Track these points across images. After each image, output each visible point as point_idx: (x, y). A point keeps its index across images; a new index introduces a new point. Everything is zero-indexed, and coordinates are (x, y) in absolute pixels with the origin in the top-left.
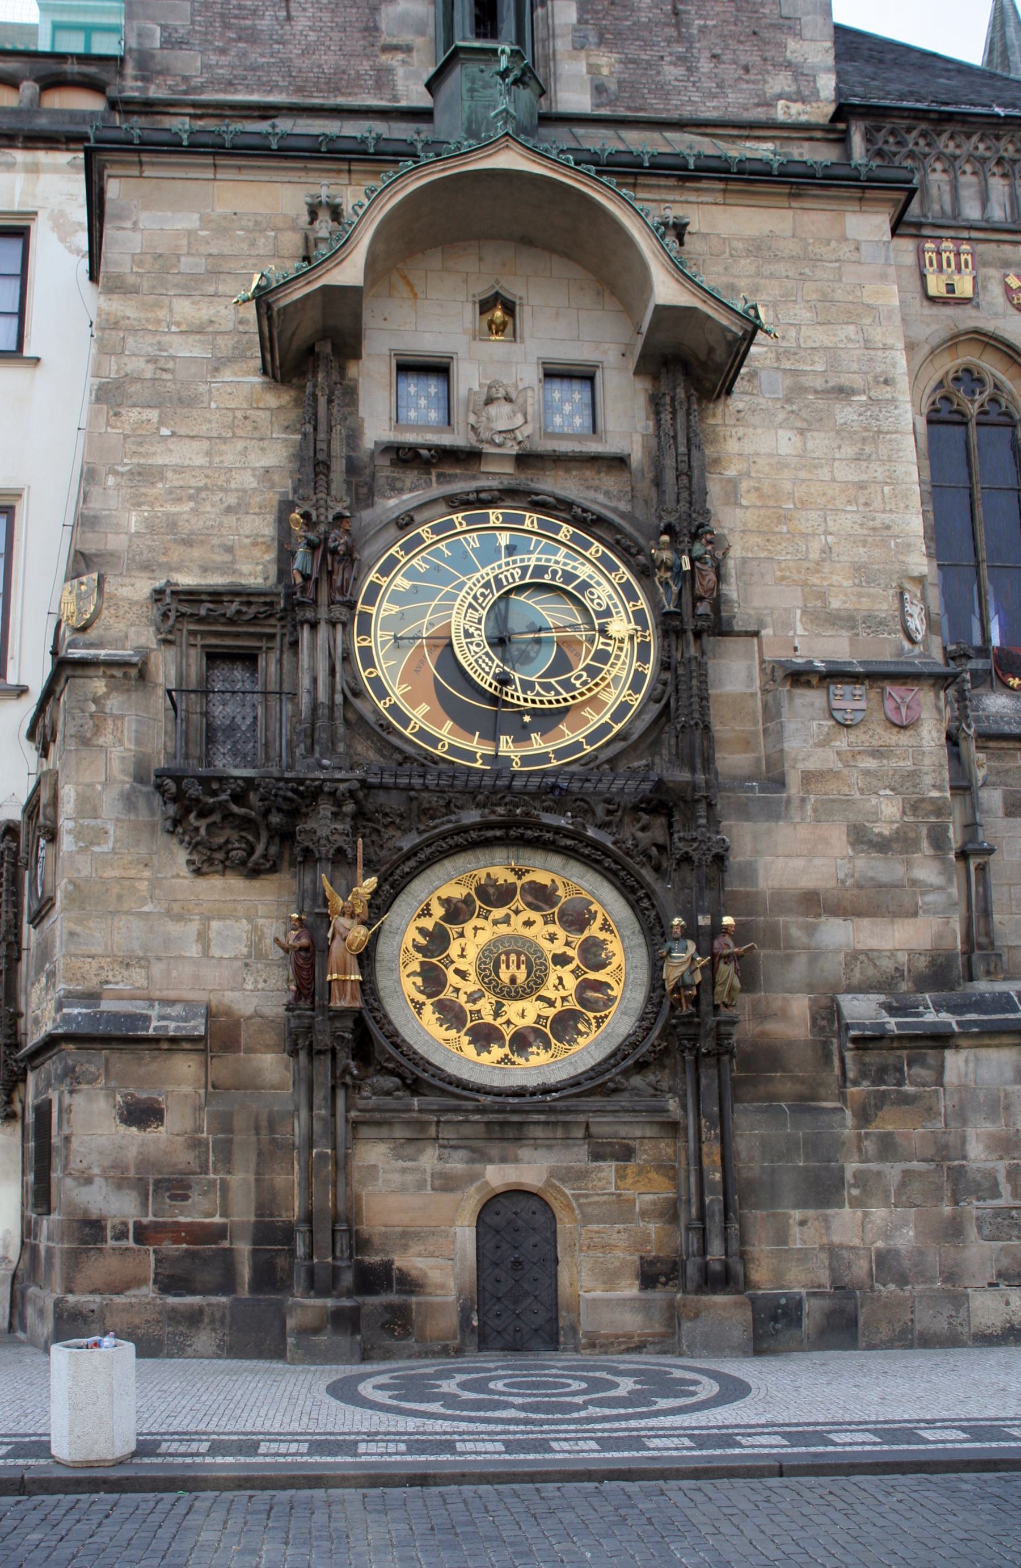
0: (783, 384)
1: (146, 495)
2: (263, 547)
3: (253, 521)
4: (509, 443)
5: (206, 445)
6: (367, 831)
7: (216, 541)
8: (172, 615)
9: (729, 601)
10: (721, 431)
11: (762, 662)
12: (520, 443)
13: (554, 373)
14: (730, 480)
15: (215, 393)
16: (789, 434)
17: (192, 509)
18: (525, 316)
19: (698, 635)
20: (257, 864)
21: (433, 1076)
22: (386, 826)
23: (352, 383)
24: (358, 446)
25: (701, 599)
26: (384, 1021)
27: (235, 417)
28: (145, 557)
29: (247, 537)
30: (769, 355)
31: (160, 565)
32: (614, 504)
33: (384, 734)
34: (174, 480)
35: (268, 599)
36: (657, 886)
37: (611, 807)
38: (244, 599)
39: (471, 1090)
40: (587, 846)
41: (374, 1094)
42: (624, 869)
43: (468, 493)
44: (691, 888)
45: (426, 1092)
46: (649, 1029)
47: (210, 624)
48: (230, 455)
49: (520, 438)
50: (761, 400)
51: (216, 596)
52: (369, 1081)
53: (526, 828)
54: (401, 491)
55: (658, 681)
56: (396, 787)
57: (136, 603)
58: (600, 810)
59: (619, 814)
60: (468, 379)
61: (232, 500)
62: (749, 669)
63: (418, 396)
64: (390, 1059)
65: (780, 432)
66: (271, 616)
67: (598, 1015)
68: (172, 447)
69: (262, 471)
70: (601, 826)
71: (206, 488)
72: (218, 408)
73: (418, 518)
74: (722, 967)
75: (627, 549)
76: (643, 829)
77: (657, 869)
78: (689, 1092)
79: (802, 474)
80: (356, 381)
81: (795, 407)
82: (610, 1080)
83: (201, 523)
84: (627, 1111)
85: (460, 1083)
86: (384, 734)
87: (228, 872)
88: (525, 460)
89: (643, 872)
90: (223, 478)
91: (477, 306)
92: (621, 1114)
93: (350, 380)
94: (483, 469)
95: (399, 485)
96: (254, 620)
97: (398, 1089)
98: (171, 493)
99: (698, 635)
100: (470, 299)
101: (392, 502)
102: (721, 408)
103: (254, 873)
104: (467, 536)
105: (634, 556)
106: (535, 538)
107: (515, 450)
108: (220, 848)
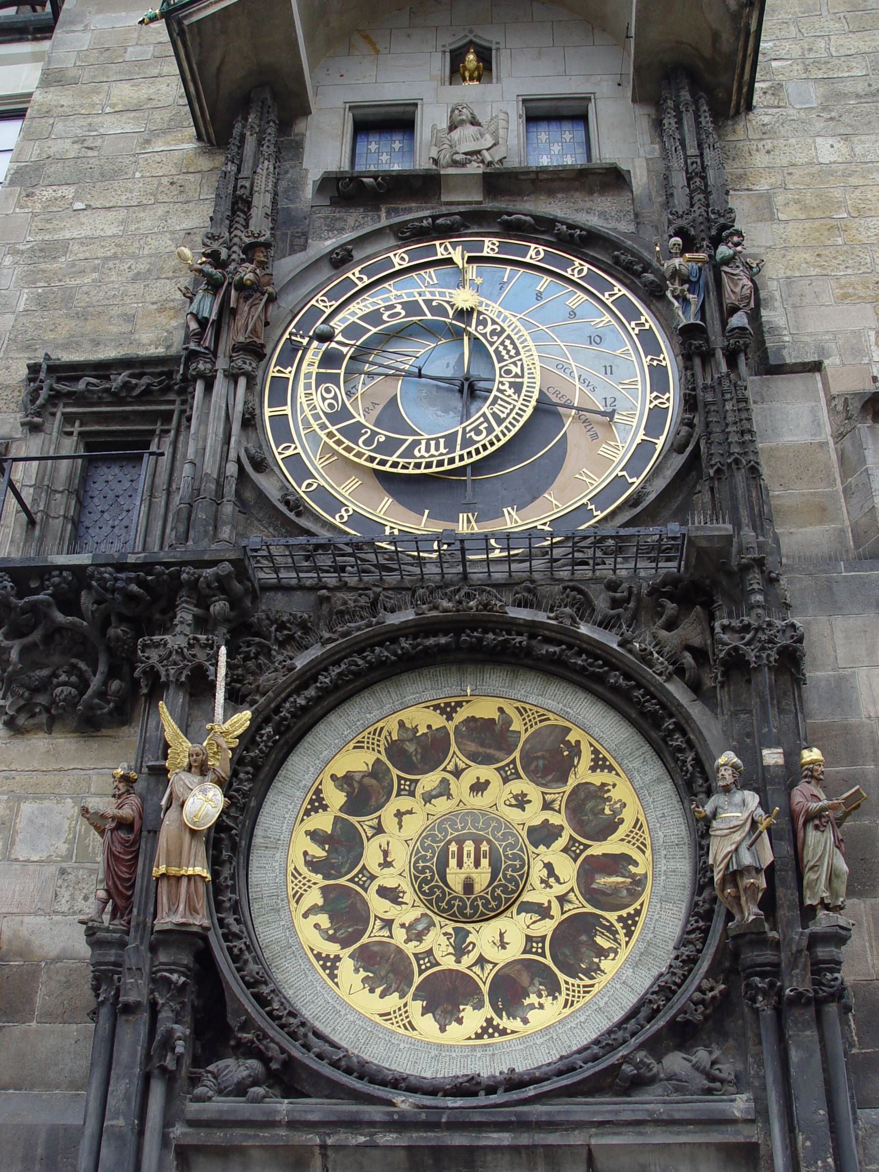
0: (815, 94)
1: (44, 271)
2: (172, 313)
3: (165, 285)
4: (475, 165)
5: (123, 213)
6: (253, 650)
7: (116, 311)
8: (44, 394)
9: (774, 330)
10: (744, 146)
11: (831, 399)
12: (490, 164)
13: (540, 114)
14: (761, 196)
15: (141, 161)
16: (831, 141)
17: (94, 281)
18: (502, 63)
19: (732, 359)
20: (90, 707)
21: (320, 1056)
22: (282, 644)
23: (298, 138)
24: (298, 197)
25: (734, 310)
26: (247, 956)
27: (160, 184)
28: (28, 337)
29: (153, 303)
30: (795, 67)
31: (45, 343)
32: (612, 224)
33: (291, 515)
34: (78, 252)
35: (165, 369)
36: (696, 710)
37: (618, 595)
38: (137, 371)
39: (384, 1083)
40: (579, 654)
41: (220, 1092)
42: (639, 686)
43: (421, 220)
44: (750, 712)
45: (307, 1088)
46: (691, 962)
47: (92, 405)
48: (148, 221)
49: (488, 158)
50: (791, 111)
51: (102, 369)
52: (209, 1068)
53: (486, 631)
54: (342, 230)
55: (683, 423)
56: (301, 588)
57: (8, 386)
58: (601, 602)
59: (632, 605)
60: (431, 120)
61: (142, 266)
62: (813, 411)
63: (379, 152)
64: (248, 1024)
65: (819, 140)
66: (168, 389)
67: (624, 913)
68: (83, 220)
69: (182, 234)
70: (606, 624)
71: (115, 257)
72: (142, 177)
73: (357, 255)
74: (812, 836)
75: (628, 268)
76: (670, 626)
77: (696, 687)
78: (770, 1079)
79: (854, 181)
80: (304, 135)
81: (833, 114)
82: (625, 1059)
83: (102, 294)
84: (658, 1122)
85: (364, 1071)
86: (291, 515)
87: (57, 727)
88: (500, 181)
89: (669, 687)
90: (136, 245)
91: (448, 55)
92: (649, 1129)
93: (297, 135)
94: (444, 198)
95: (338, 225)
96: (146, 395)
97: (255, 1083)
98: (74, 266)
99: (732, 359)
100: (440, 49)
101: (329, 242)
102: (742, 124)
103: (91, 724)
104: (422, 272)
105: (638, 275)
106: (509, 268)
107: (480, 171)
108: (45, 686)
